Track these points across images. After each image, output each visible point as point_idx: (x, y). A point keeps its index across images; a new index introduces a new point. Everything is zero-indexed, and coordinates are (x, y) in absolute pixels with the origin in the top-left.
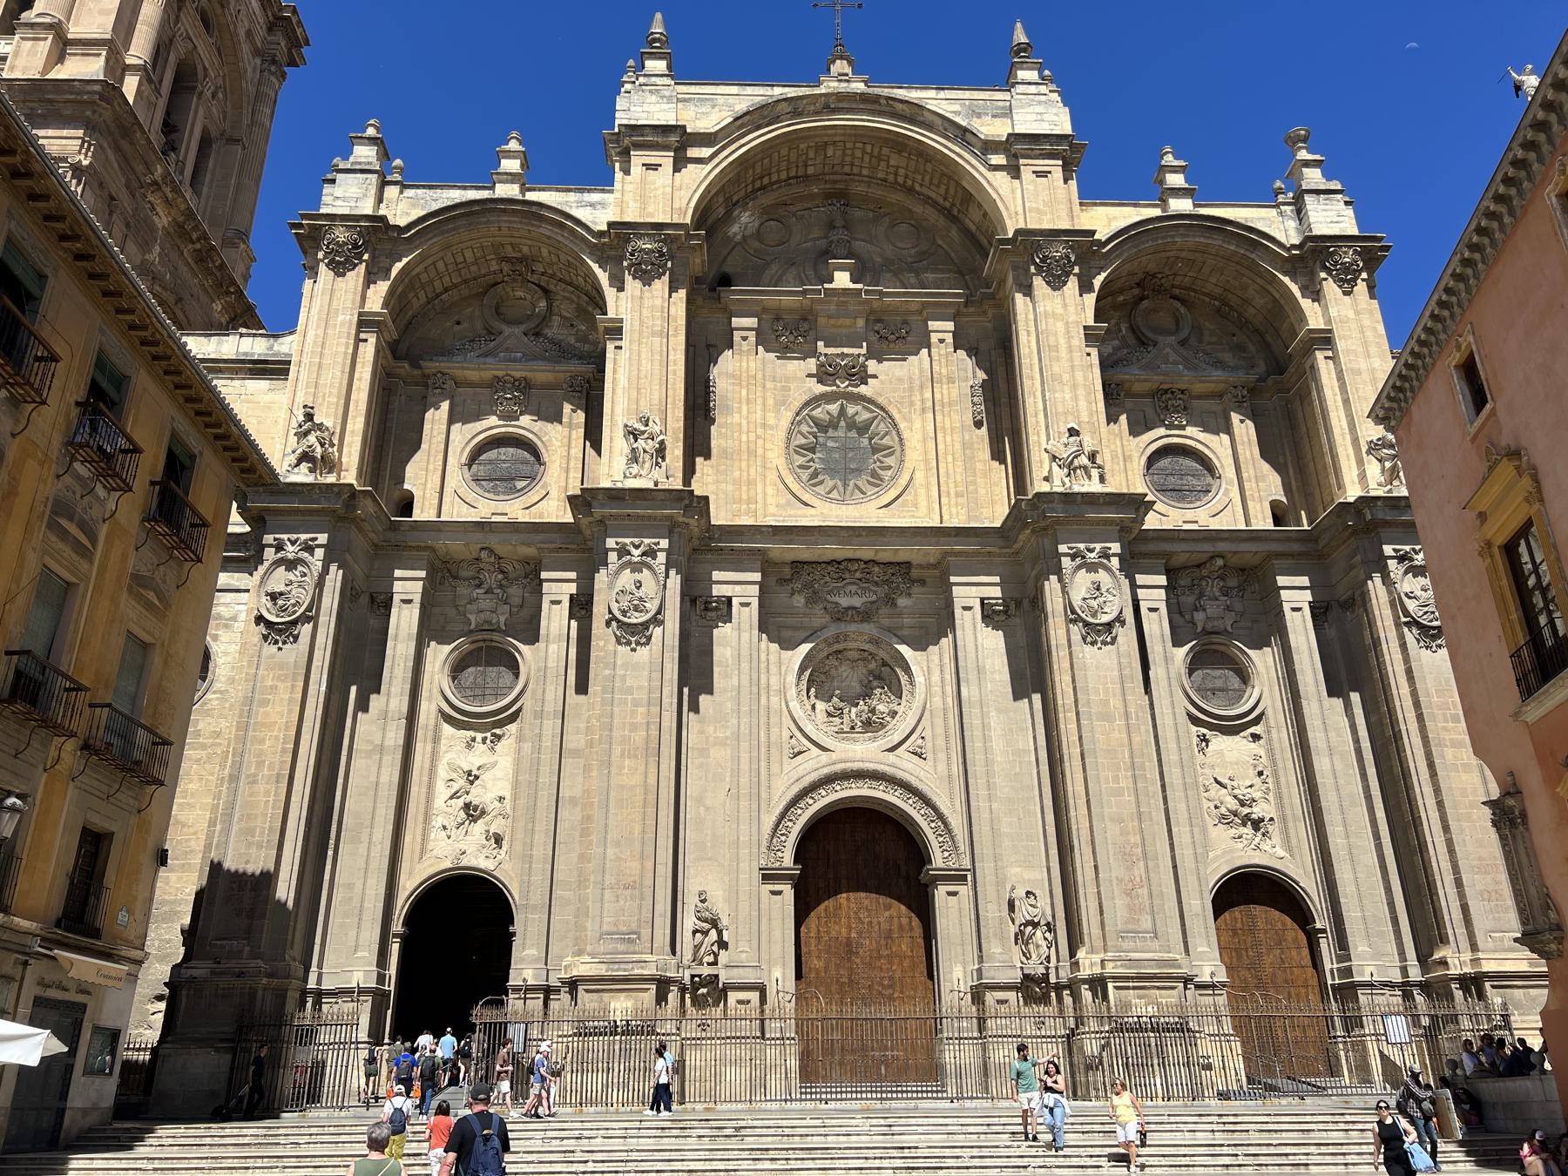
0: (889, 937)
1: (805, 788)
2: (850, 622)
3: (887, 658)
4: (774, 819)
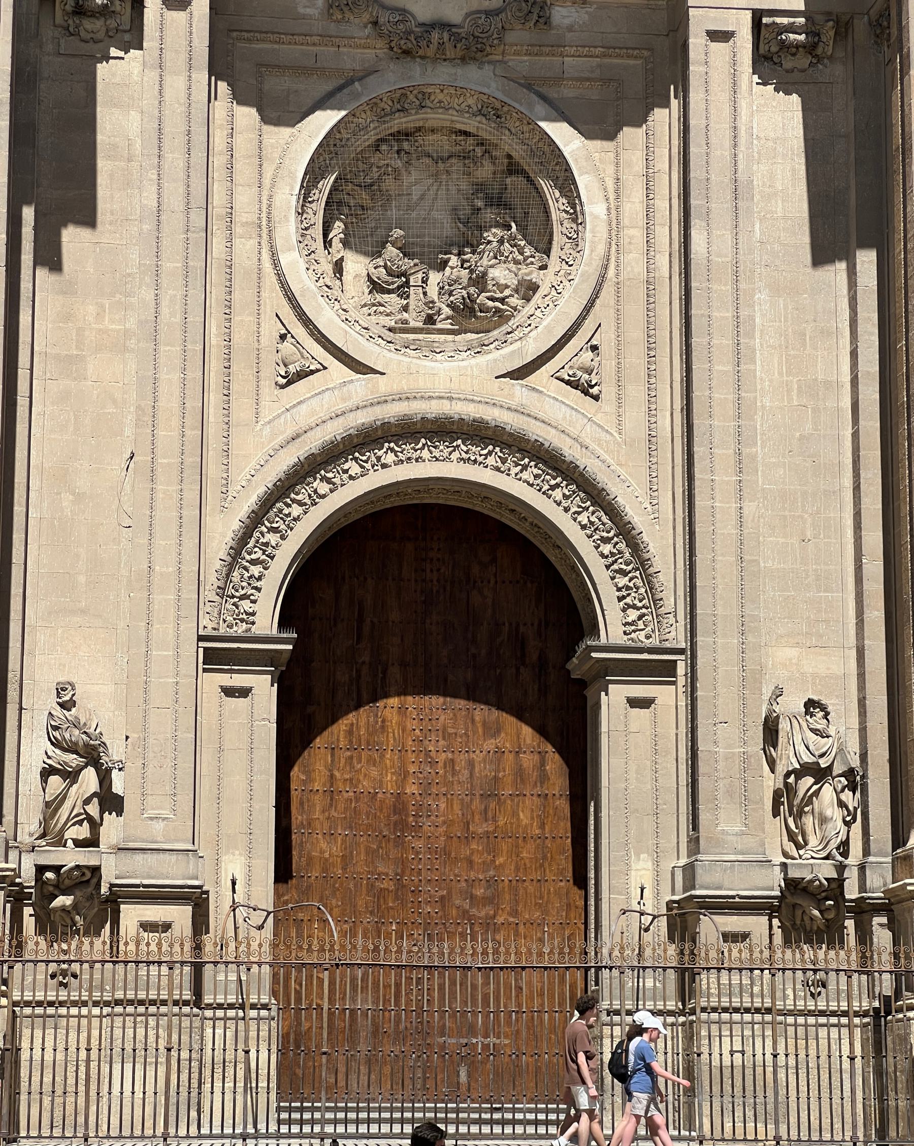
1: (311, 458)
2: (435, 60)
3: (518, 152)
4: (236, 525)
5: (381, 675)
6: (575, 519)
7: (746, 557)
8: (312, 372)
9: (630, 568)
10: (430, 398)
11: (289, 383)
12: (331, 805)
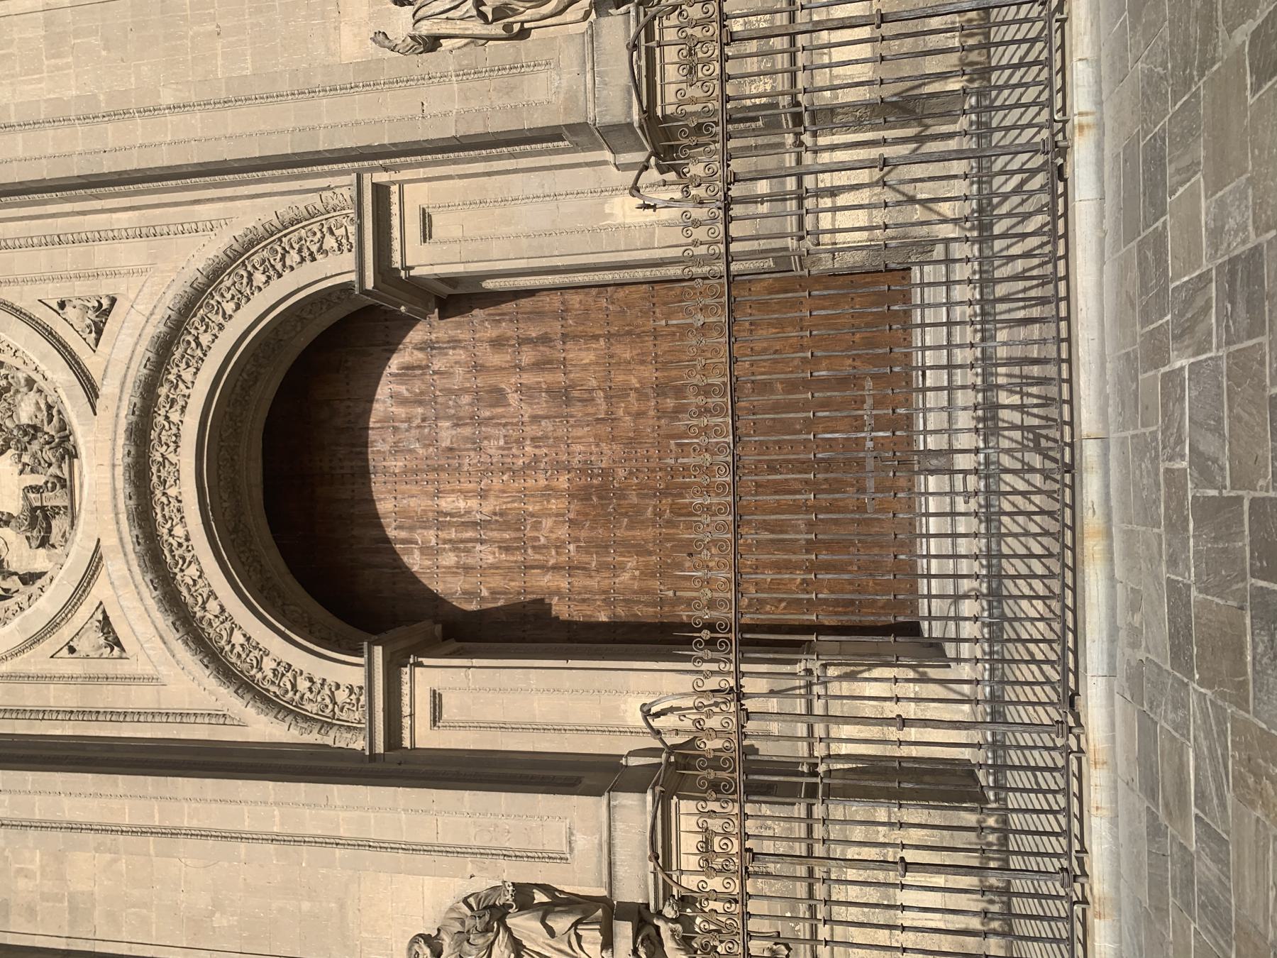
0: (562, 395)
5: (448, 519)
6: (231, 317)
7: (223, 96)
8: (106, 618)
9: (279, 249)
10: (115, 489)
11: (118, 643)
12: (584, 569)
